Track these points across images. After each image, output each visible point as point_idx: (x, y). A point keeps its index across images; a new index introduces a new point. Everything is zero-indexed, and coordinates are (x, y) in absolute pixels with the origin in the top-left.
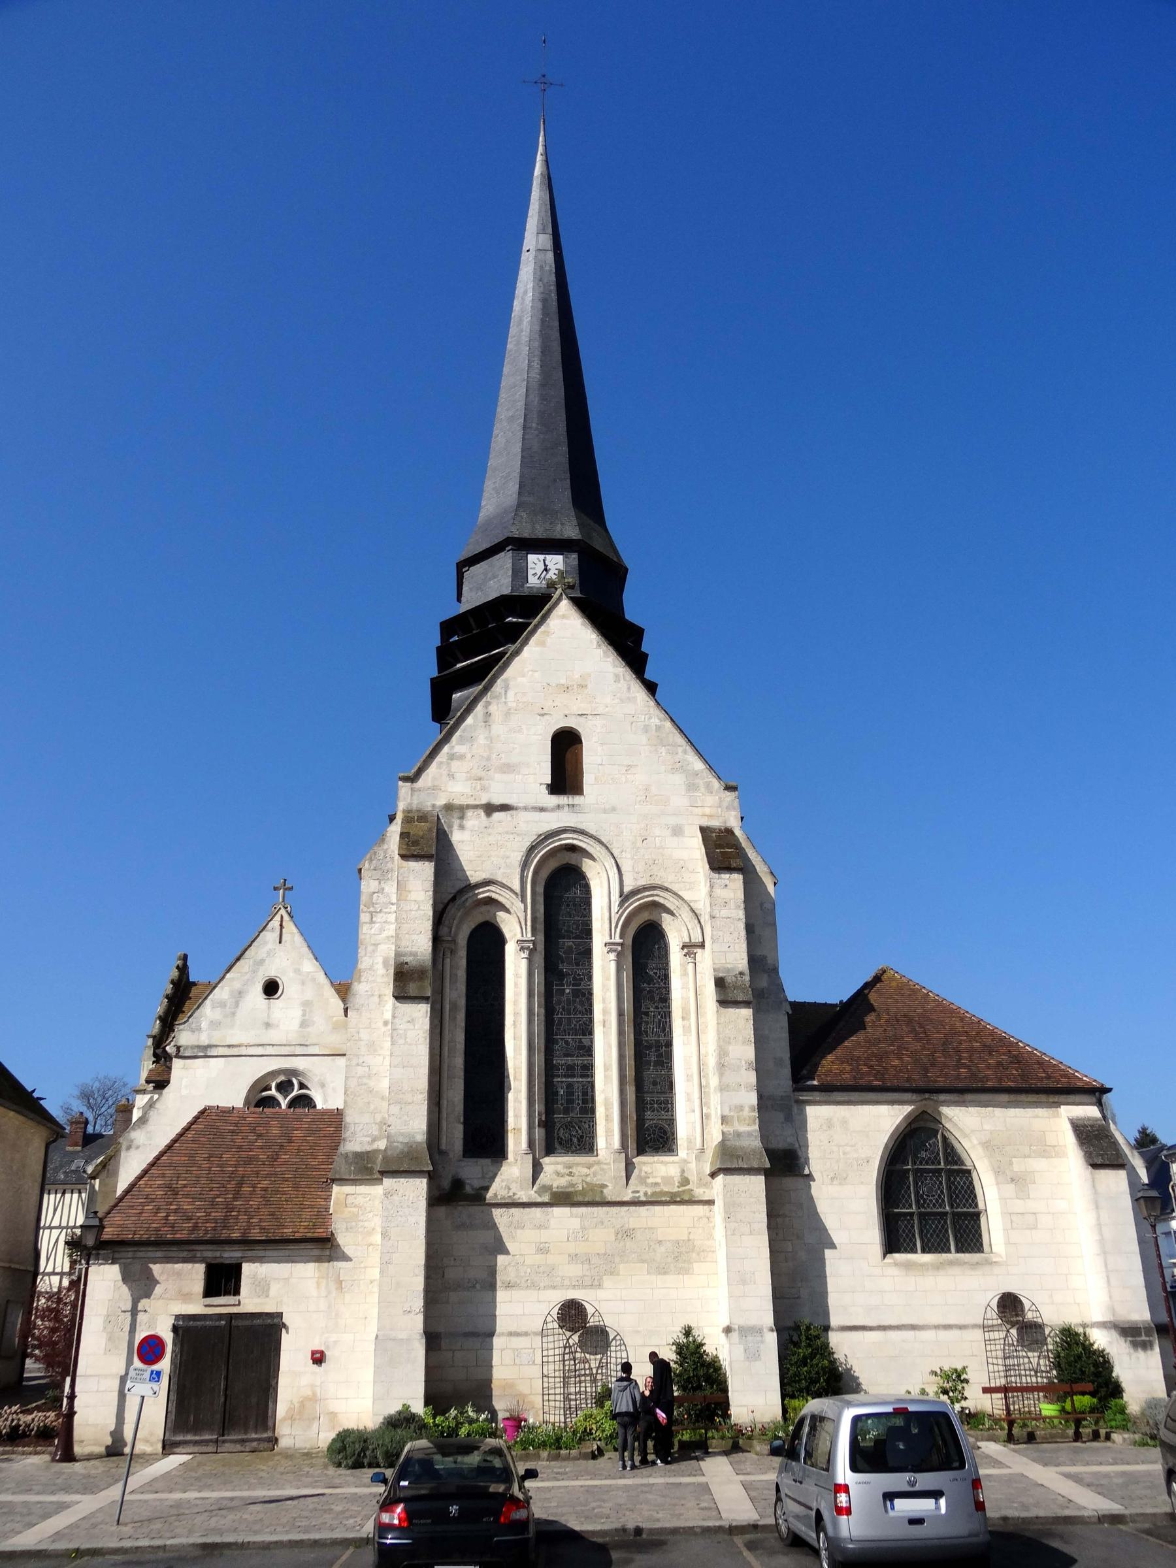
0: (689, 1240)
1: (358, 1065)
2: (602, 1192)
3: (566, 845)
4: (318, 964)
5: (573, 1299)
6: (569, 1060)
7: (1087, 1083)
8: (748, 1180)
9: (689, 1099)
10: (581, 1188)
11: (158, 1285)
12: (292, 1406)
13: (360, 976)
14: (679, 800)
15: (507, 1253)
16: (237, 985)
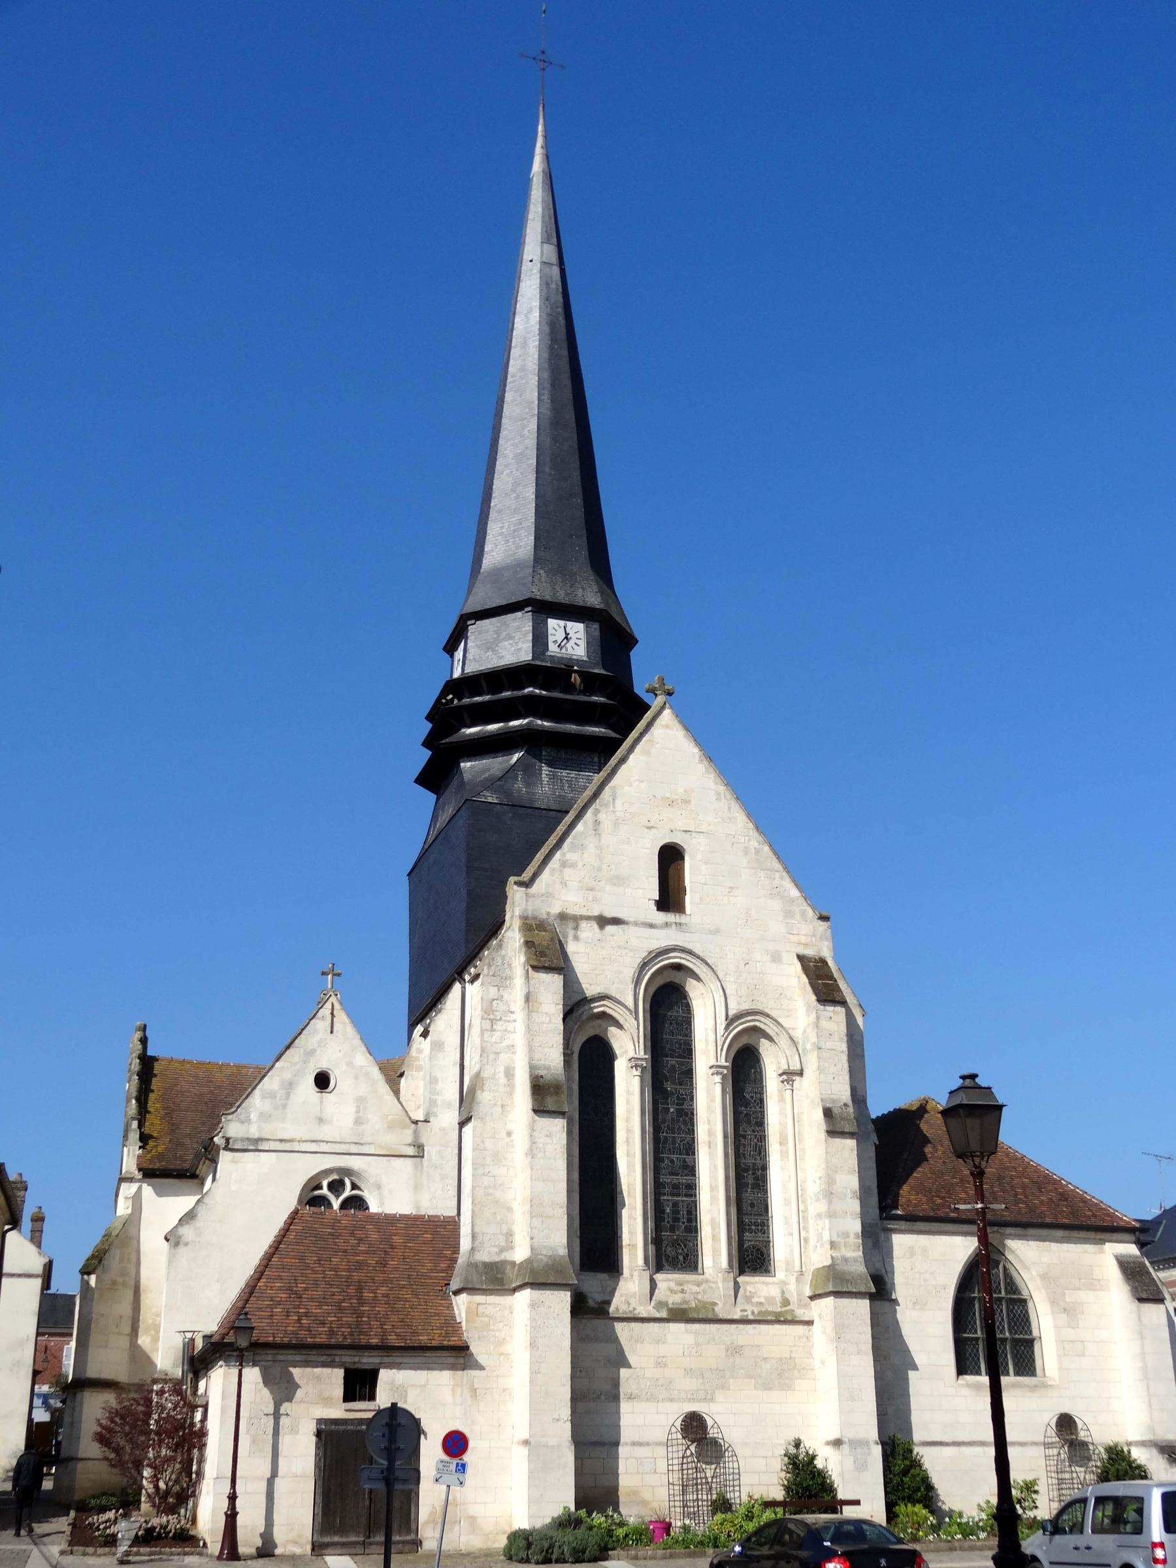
0: (791, 1358)
1: (483, 1174)
2: (713, 1310)
3: (673, 964)
4: (371, 1058)
5: (694, 1412)
6: (675, 1179)
7: (1129, 1223)
8: (855, 1304)
9: (787, 1221)
10: (694, 1305)
11: (299, 1390)
12: (434, 1510)
13: (483, 1084)
14: (777, 927)
15: (629, 1366)
16: (287, 1076)
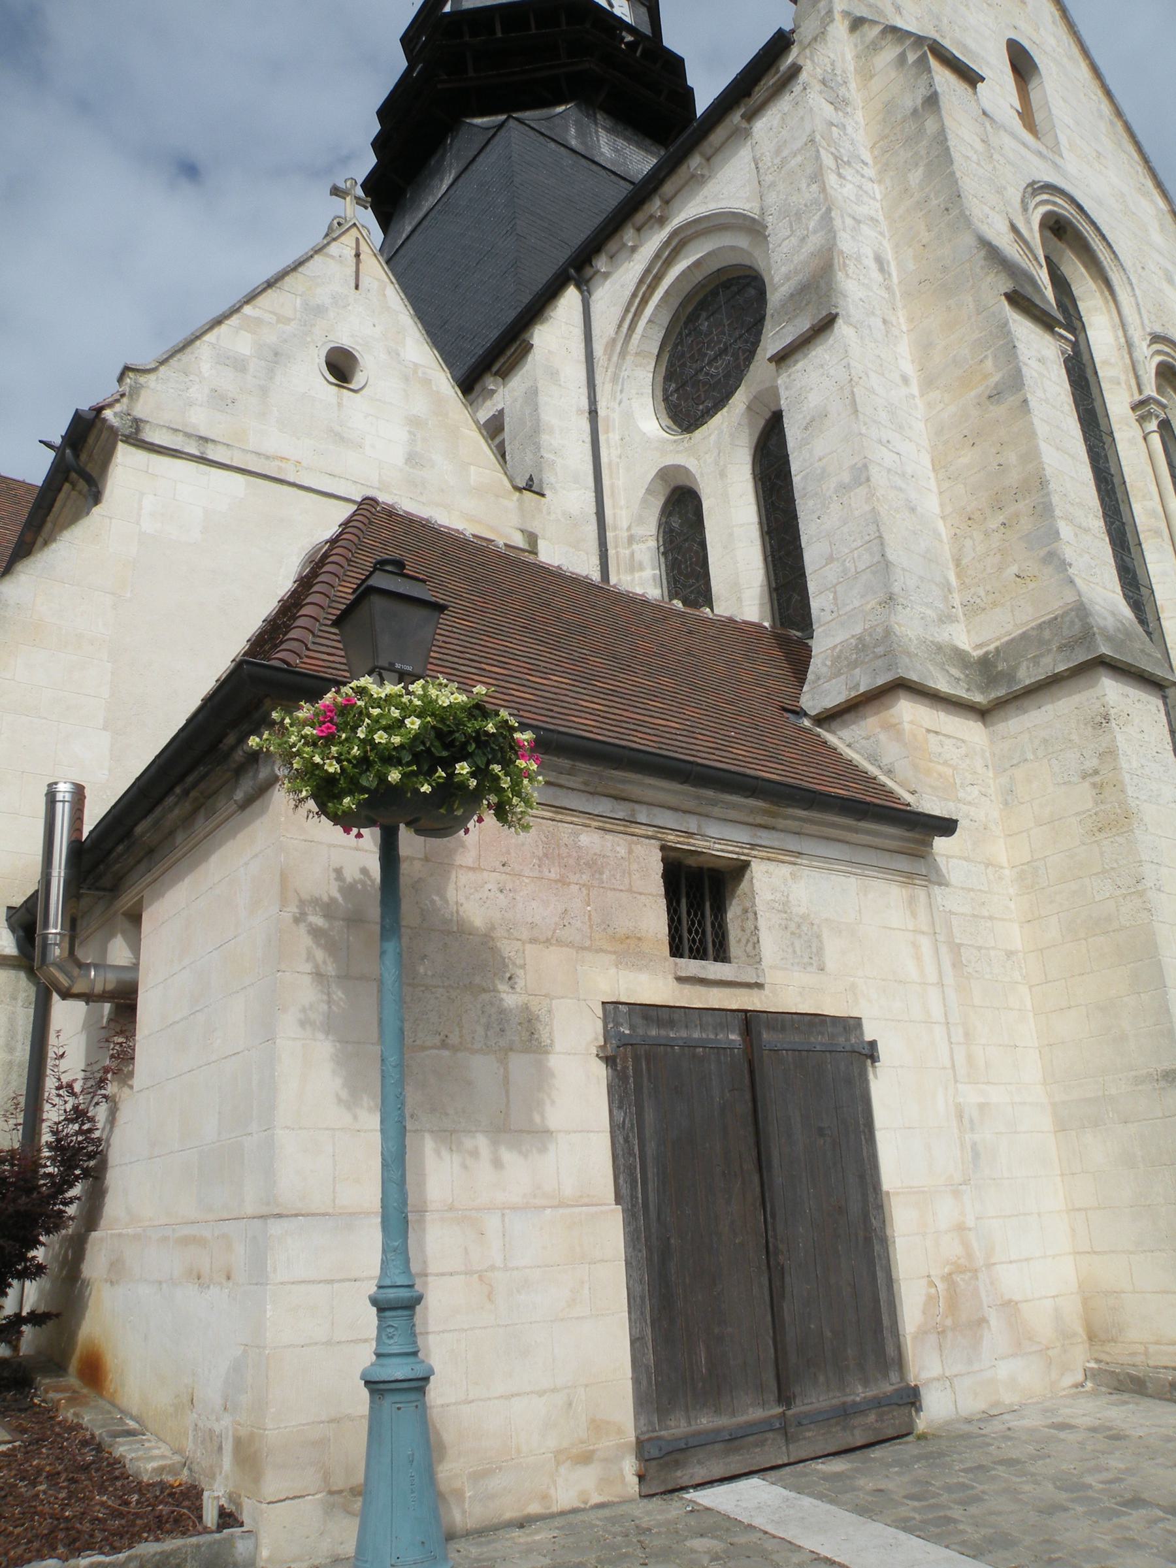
1: (880, 442)
16: (270, 337)
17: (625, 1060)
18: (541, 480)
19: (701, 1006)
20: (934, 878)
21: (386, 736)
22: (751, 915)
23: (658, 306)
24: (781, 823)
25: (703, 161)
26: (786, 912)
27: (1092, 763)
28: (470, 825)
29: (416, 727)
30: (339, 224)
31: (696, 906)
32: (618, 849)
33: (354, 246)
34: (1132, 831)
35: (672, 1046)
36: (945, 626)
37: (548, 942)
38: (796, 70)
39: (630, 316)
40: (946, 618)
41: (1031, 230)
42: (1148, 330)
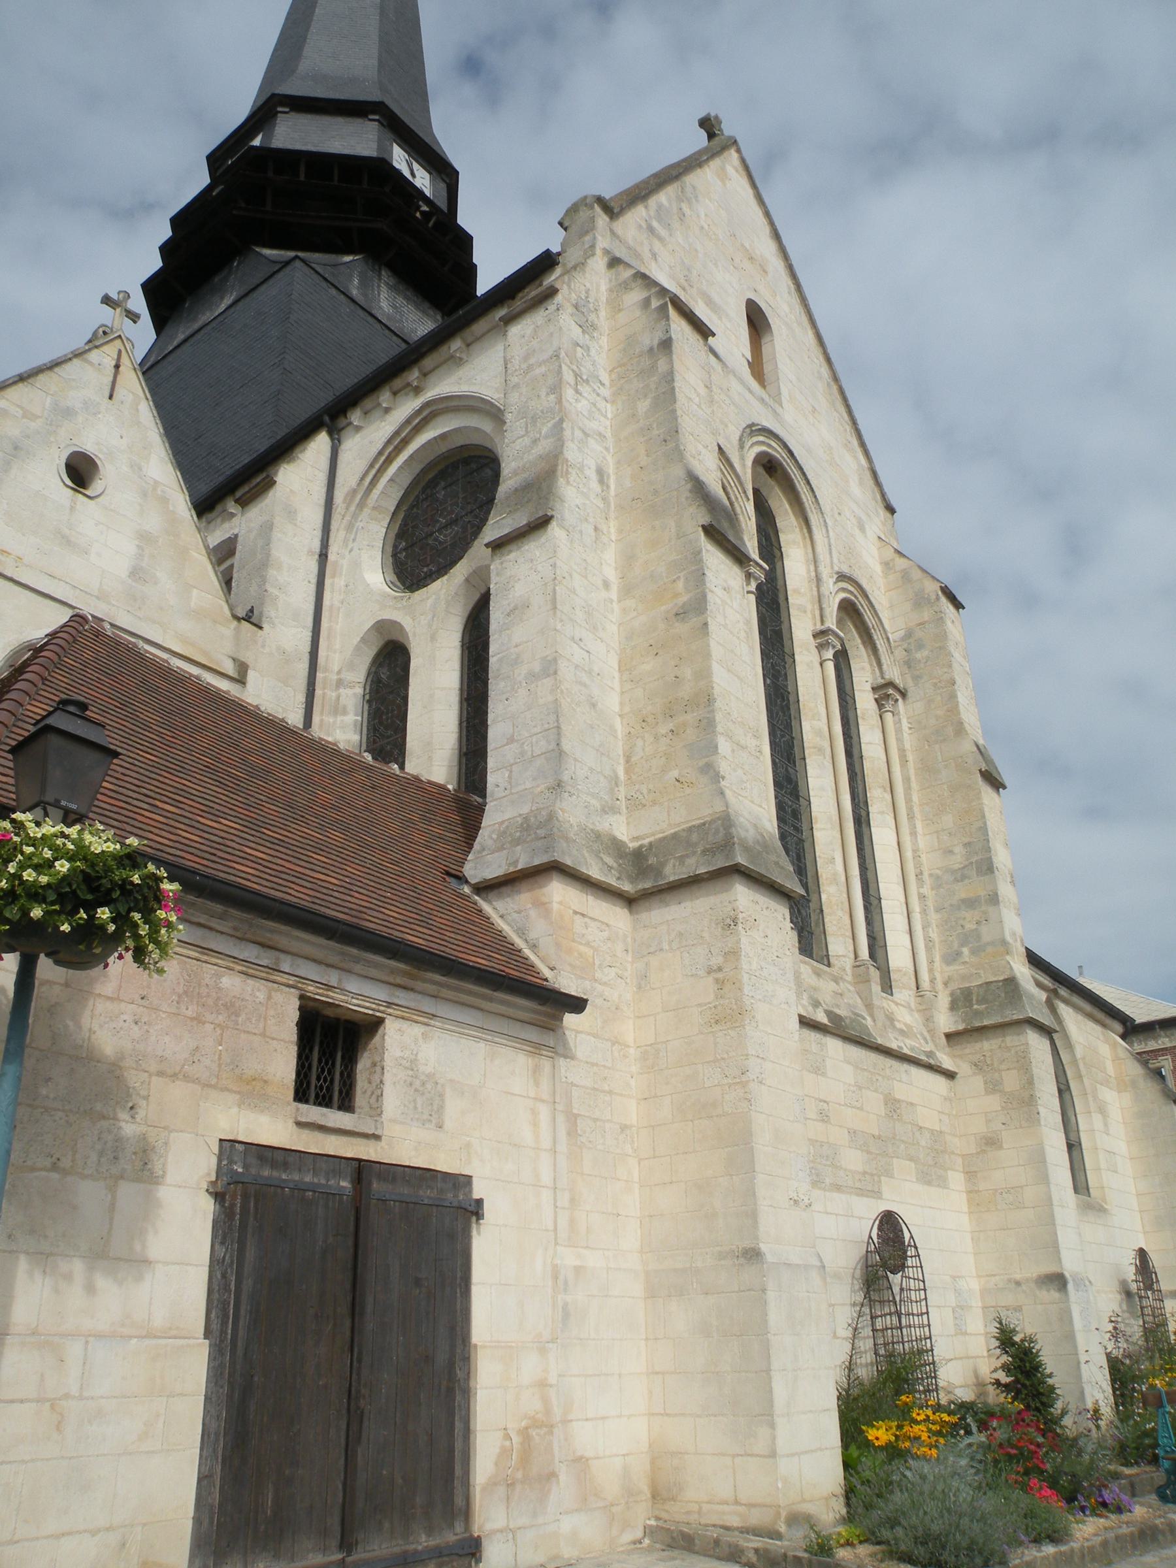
1: (573, 639)
17: (234, 1197)
18: (261, 614)
19: (317, 1152)
20: (560, 1050)
21: (34, 874)
22: (378, 1069)
23: (401, 468)
24: (419, 985)
25: (463, 346)
26: (412, 1070)
27: (717, 960)
28: (111, 960)
29: (65, 870)
30: (105, 333)
31: (327, 1056)
32: (258, 994)
33: (116, 357)
34: (743, 1026)
35: (283, 1188)
36: (607, 816)
37: (174, 1076)
38: (552, 292)
39: (373, 472)
40: (609, 809)
41: (744, 466)
42: (836, 569)
